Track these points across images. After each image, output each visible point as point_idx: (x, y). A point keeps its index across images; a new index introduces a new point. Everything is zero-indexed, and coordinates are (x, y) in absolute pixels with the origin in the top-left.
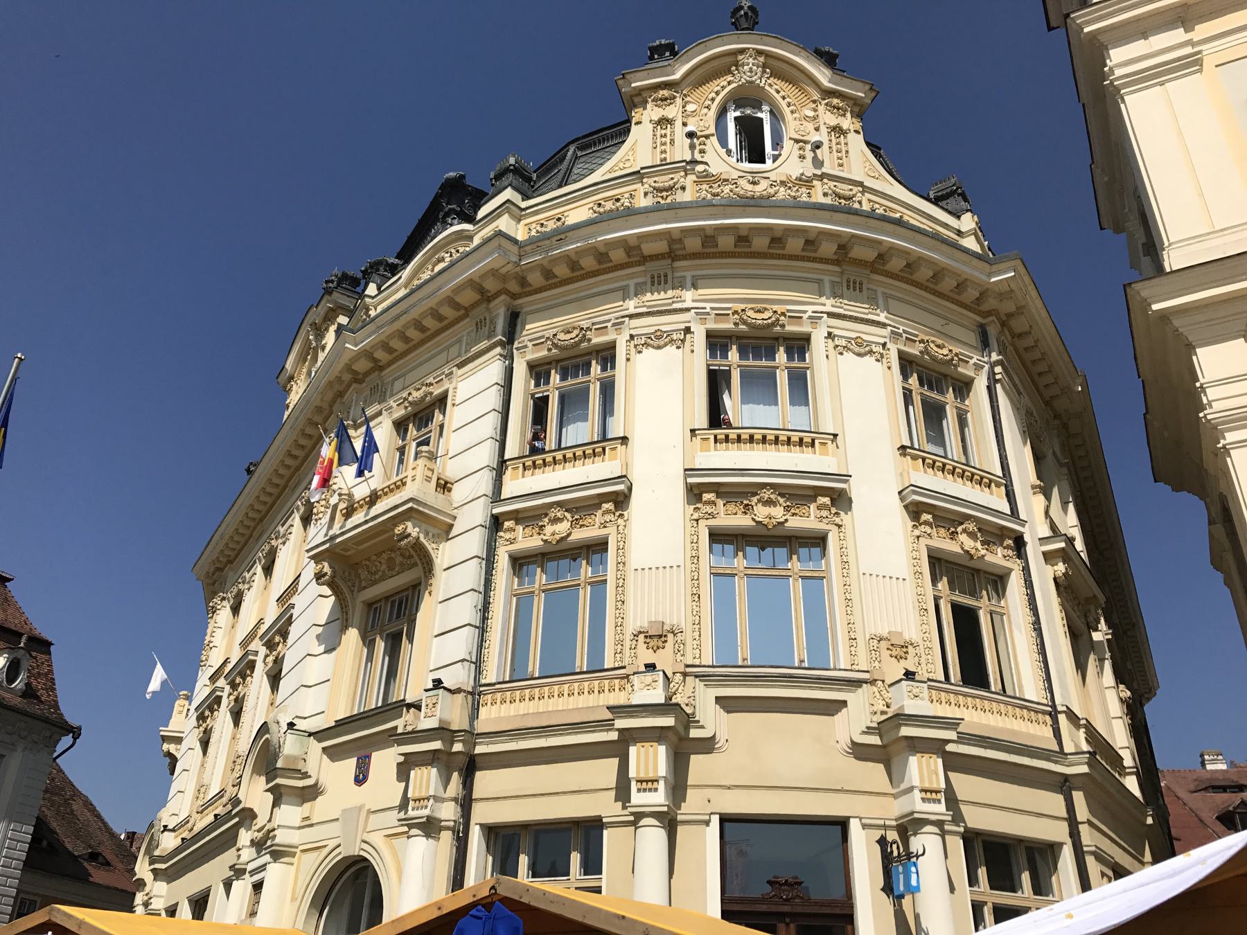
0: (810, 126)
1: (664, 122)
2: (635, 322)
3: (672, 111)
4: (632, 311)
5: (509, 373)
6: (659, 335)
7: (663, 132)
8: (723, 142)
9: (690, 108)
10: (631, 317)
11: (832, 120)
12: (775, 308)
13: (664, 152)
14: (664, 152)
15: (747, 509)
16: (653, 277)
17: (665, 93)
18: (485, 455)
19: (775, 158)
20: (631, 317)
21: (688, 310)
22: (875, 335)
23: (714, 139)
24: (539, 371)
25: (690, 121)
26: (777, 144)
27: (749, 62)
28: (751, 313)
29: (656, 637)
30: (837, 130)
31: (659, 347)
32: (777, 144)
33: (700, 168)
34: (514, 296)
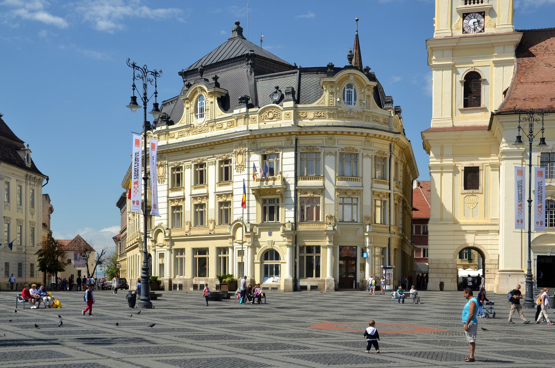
2: (326, 149)
3: (334, 90)
6: (330, 153)
8: (344, 100)
9: (338, 89)
10: (324, 147)
11: (367, 93)
15: (346, 193)
18: (292, 174)
19: (355, 104)
20: (324, 147)
26: (355, 100)
27: (352, 77)
29: (331, 217)
30: (369, 96)
32: (355, 100)
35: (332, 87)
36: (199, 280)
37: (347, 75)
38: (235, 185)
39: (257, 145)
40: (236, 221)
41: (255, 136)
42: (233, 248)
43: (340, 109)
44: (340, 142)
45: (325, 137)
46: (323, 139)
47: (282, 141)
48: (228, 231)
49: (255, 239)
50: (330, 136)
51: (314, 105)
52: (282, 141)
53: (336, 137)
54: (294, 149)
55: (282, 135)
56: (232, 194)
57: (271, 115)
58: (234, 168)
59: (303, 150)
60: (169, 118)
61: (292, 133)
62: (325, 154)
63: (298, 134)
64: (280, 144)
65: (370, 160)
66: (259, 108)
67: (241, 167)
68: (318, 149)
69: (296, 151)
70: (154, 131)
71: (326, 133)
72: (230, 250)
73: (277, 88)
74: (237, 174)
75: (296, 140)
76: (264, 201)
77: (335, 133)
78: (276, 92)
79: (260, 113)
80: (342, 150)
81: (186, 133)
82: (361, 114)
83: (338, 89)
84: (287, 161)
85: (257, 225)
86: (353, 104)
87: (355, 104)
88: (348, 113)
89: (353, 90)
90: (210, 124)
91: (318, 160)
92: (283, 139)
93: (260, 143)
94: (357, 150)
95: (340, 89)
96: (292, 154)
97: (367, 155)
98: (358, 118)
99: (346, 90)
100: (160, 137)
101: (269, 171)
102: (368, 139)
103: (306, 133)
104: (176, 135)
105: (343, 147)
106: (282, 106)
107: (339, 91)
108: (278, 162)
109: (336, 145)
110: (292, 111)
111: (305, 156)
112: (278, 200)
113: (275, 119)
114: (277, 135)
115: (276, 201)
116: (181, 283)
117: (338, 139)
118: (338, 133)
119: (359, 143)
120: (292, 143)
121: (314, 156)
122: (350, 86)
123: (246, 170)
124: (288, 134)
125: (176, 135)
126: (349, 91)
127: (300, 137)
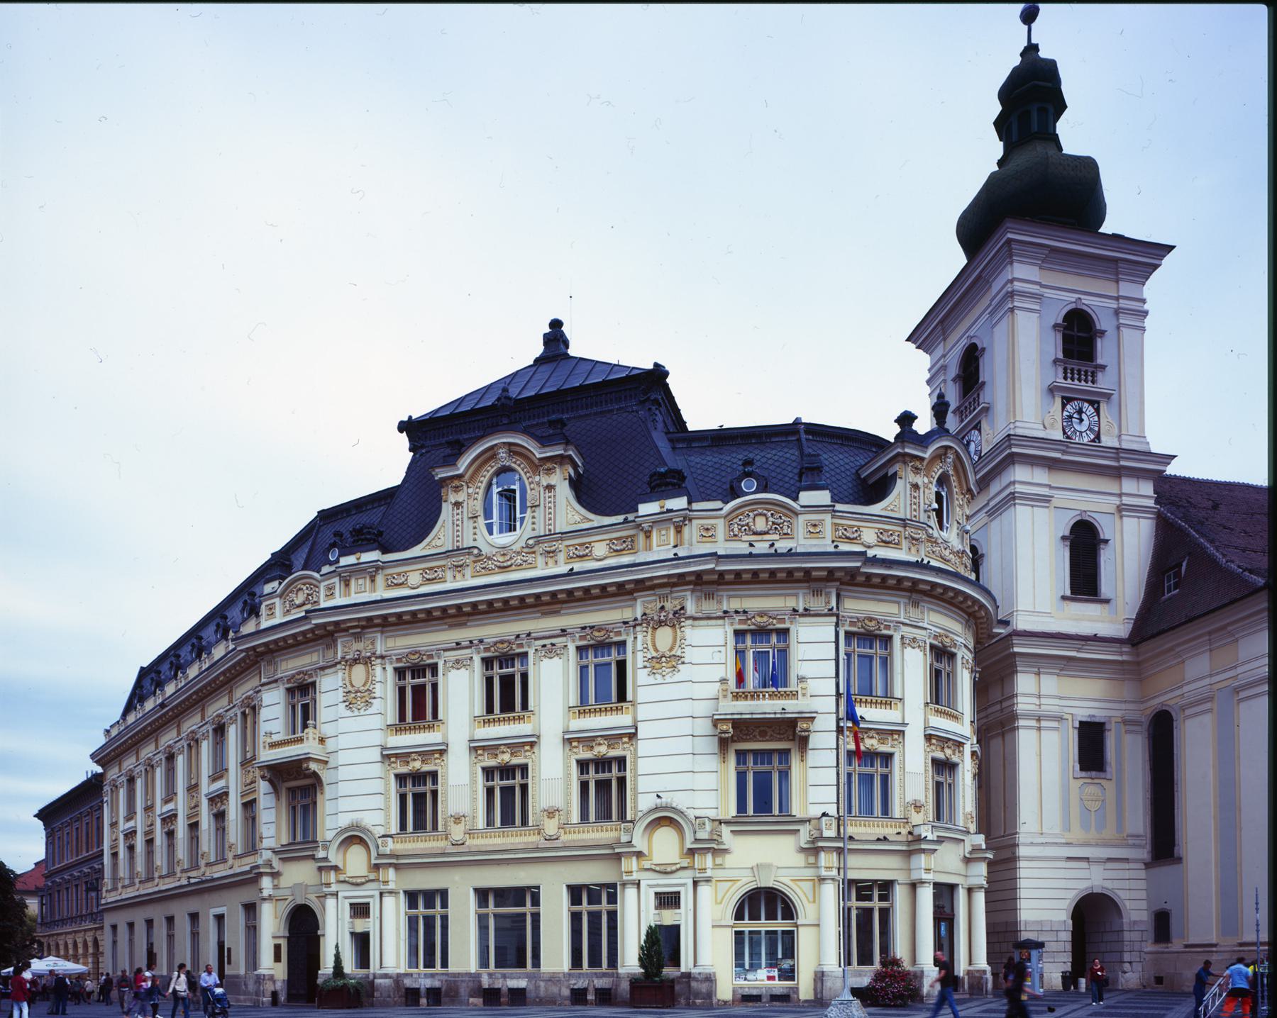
4: (902, 620)
24: (849, 635)
36: (504, 977)
38: (642, 712)
40: (651, 811)
42: (638, 884)
46: (899, 603)
48: (624, 839)
49: (719, 860)
50: (914, 596)
54: (834, 619)
56: (633, 736)
58: (640, 664)
60: (380, 534)
64: (791, 603)
67: (666, 662)
69: (837, 625)
70: (326, 569)
72: (631, 893)
74: (651, 680)
76: (741, 755)
81: (449, 574)
84: (814, 649)
85: (727, 823)
90: (539, 549)
96: (825, 630)
100: (353, 582)
101: (776, 676)
104: (415, 578)
112: (785, 754)
115: (776, 758)
116: (437, 984)
123: (685, 672)
125: (415, 578)
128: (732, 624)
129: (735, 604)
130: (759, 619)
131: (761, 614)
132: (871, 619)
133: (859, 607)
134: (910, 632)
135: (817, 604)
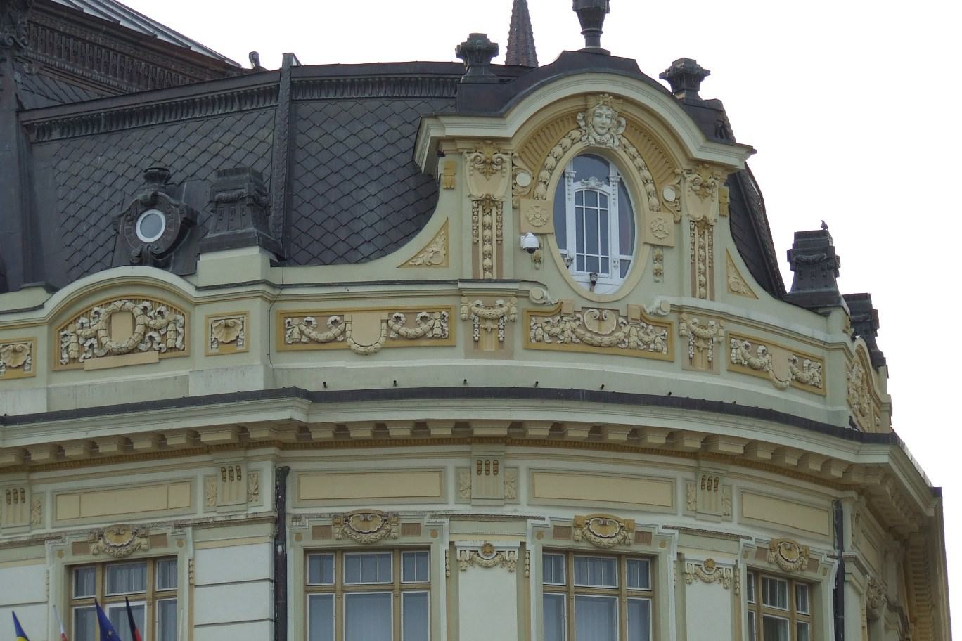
0: (668, 218)
1: (487, 203)
3: (499, 188)
4: (453, 507)
5: (280, 564)
6: (488, 549)
7: (487, 219)
8: (562, 243)
9: (524, 179)
10: (453, 517)
11: (694, 207)
12: (623, 517)
13: (488, 255)
14: (488, 255)
16: (479, 464)
17: (488, 153)
21: (523, 519)
22: (725, 557)
23: (552, 241)
25: (526, 203)
27: (603, 116)
28: (594, 528)
30: (703, 225)
31: (487, 567)
33: (536, 292)
34: (284, 446)
35: (488, 168)
37: (578, 103)
39: (37, 508)
41: (25, 451)
43: (536, 292)
44: (547, 486)
45: (453, 462)
47: (189, 481)
50: (480, 451)
51: (387, 267)
52: (189, 481)
53: (521, 463)
54: (268, 529)
55: (195, 444)
57: (122, 335)
59: (320, 531)
61: (255, 435)
62: (455, 564)
63: (291, 437)
65: (727, 594)
66: (52, 290)
68: (413, 529)
69: (279, 538)
71: (463, 433)
73: (158, 176)
75: (282, 475)
77: (517, 434)
78: (152, 203)
79: (60, 322)
80: (561, 531)
82: (666, 325)
83: (524, 179)
86: (615, 272)
87: (624, 267)
88: (586, 317)
89: (611, 191)
91: (418, 598)
92: (201, 471)
93: (57, 494)
94: (644, 537)
95: (537, 181)
97: (709, 565)
98: (645, 352)
99: (573, 187)
102: (708, 466)
103: (342, 436)
105: (570, 515)
106: (188, 272)
107: (531, 194)
108: (167, 606)
109: (523, 510)
110: (255, 310)
111: (338, 573)
113: (153, 356)
114: (161, 447)
117: (533, 472)
118: (533, 432)
119: (659, 493)
120: (253, 494)
121: (396, 571)
122: (597, 159)
124: (226, 437)
126: (591, 193)
127: (300, 462)
128: (60, 554)
129: (68, 508)
130: (111, 540)
131: (119, 530)
132: (366, 516)
133: (330, 492)
134: (470, 539)
135: (232, 498)
